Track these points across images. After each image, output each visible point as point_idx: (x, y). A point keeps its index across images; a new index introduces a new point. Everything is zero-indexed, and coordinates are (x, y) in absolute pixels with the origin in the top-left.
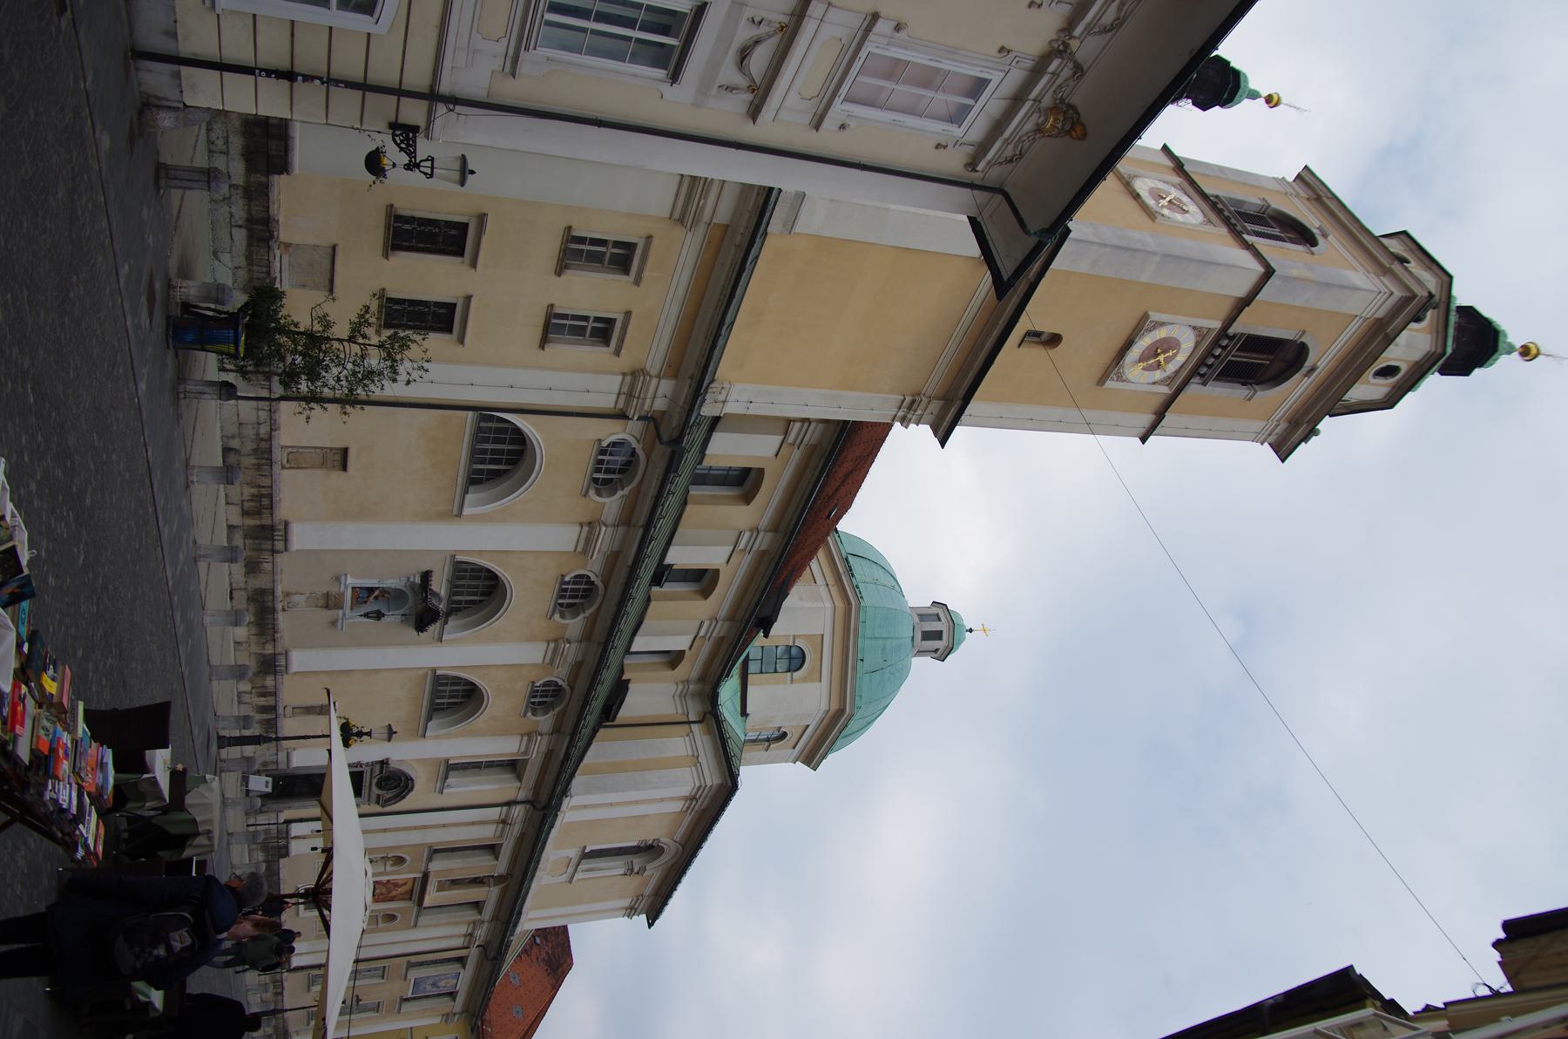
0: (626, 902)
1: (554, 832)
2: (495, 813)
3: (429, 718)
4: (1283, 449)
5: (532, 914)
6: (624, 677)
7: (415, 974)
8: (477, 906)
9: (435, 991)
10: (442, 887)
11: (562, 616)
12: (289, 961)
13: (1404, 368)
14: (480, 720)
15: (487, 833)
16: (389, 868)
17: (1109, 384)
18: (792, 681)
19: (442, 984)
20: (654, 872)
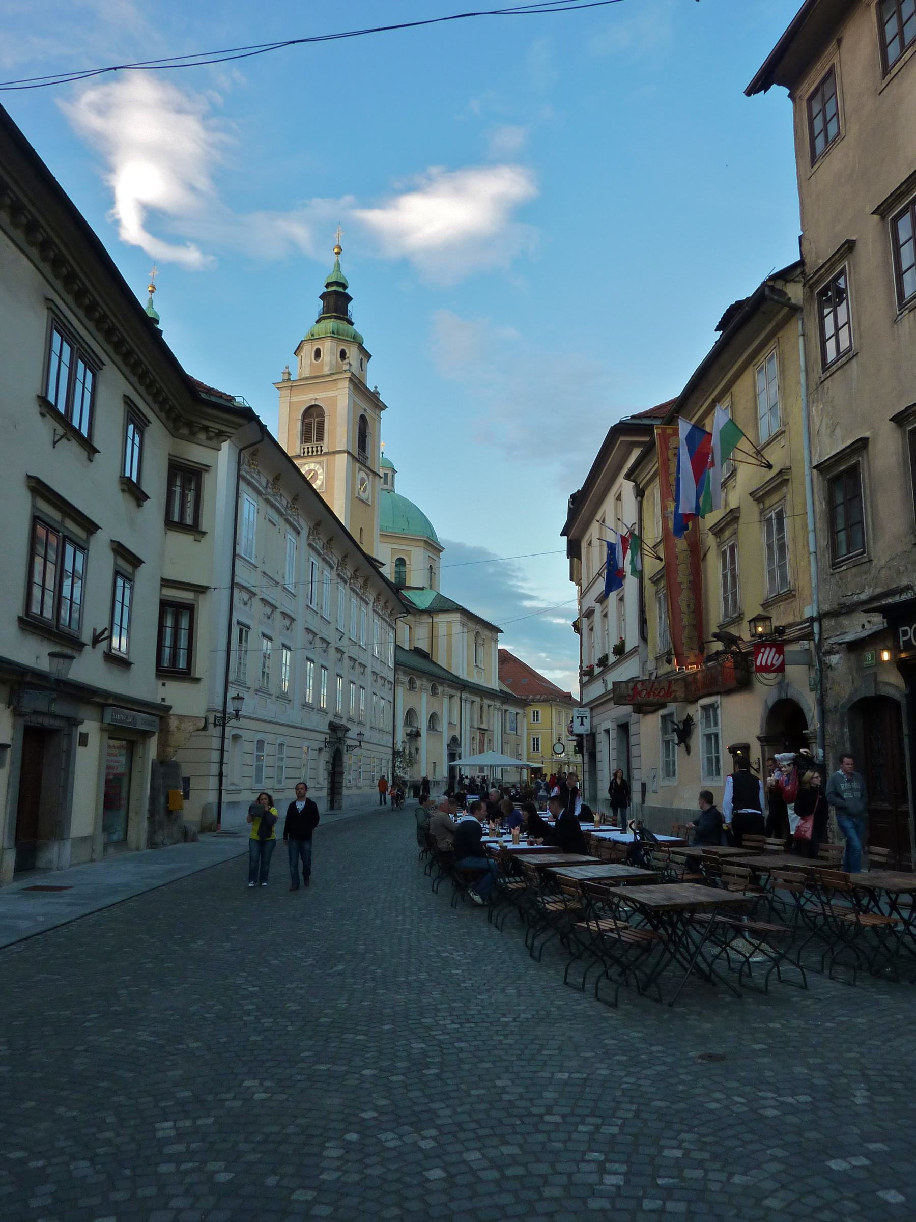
0: (493, 643)
1: (469, 680)
2: (463, 704)
3: (436, 730)
4: (383, 407)
5: (493, 684)
6: (413, 649)
7: (508, 731)
8: (489, 706)
9: (515, 722)
10: (482, 722)
11: (416, 688)
12: (500, 779)
13: (361, 356)
14: (439, 713)
15: (468, 706)
16: (475, 743)
17: (370, 503)
18: (410, 565)
19: (513, 719)
20: (485, 633)
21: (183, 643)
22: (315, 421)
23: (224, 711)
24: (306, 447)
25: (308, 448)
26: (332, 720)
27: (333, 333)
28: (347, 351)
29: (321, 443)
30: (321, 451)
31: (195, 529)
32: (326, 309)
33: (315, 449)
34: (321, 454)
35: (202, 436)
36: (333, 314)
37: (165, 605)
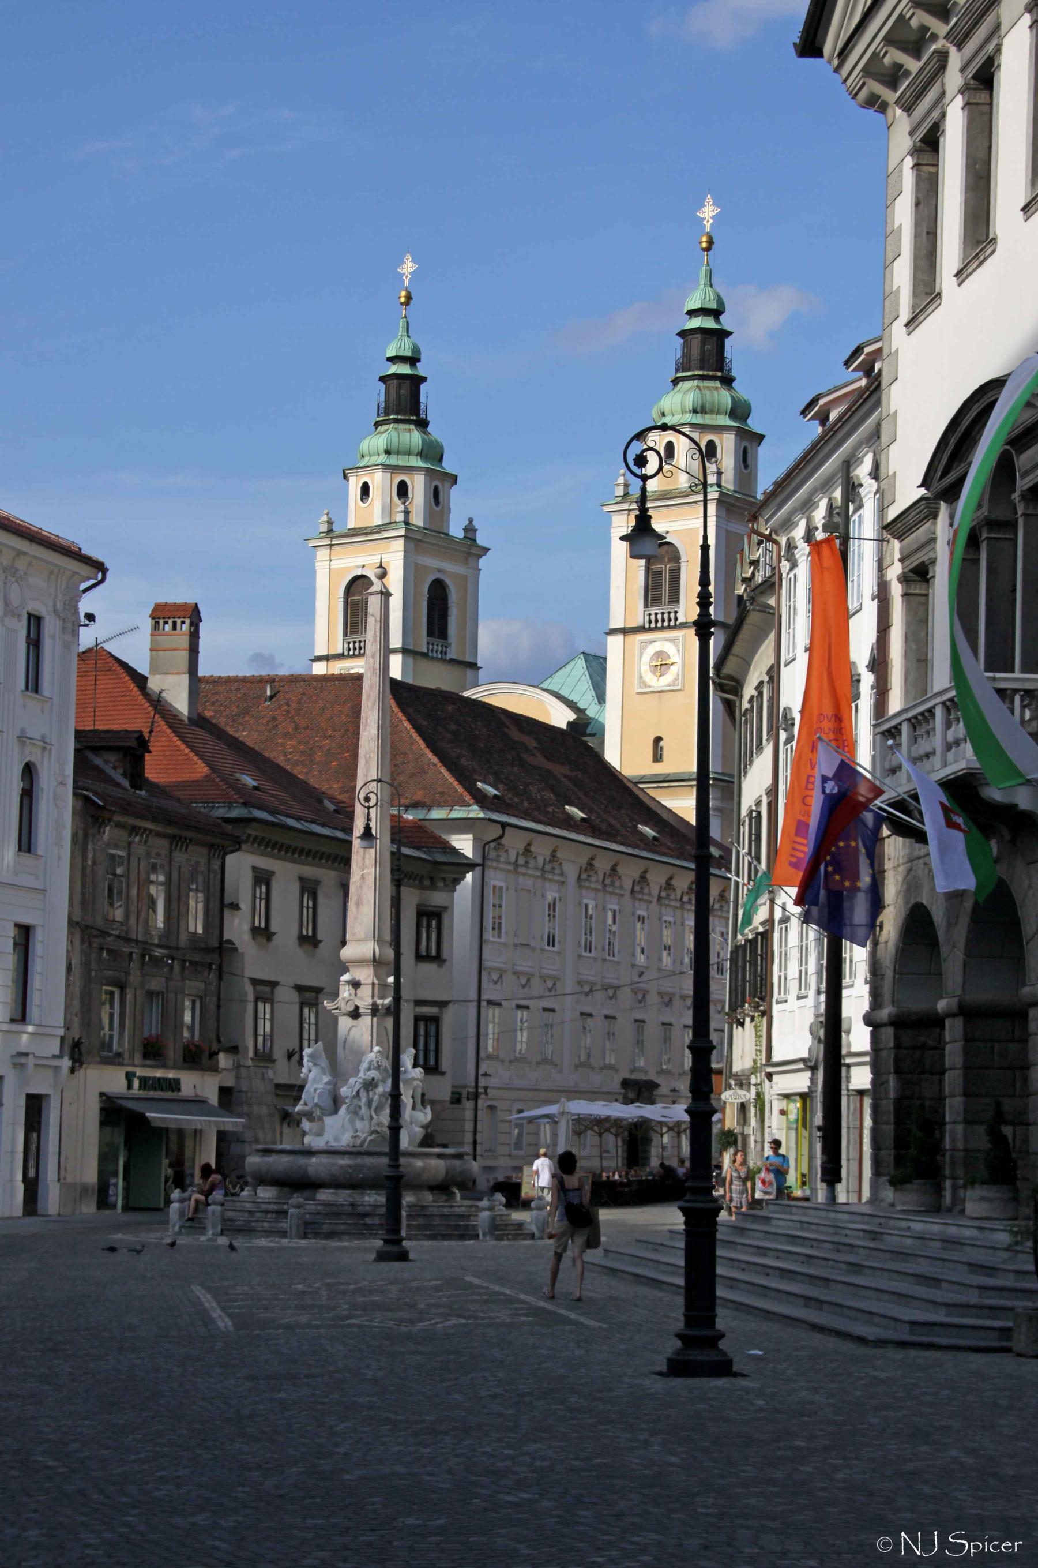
21: (432, 1047)
22: (666, 568)
23: (477, 1087)
24: (653, 612)
25: (656, 614)
26: (627, 1076)
27: (695, 411)
28: (718, 443)
29: (674, 607)
30: (676, 619)
31: (438, 959)
32: (684, 364)
33: (666, 616)
34: (676, 627)
35: (440, 884)
36: (696, 373)
37: (417, 1019)
